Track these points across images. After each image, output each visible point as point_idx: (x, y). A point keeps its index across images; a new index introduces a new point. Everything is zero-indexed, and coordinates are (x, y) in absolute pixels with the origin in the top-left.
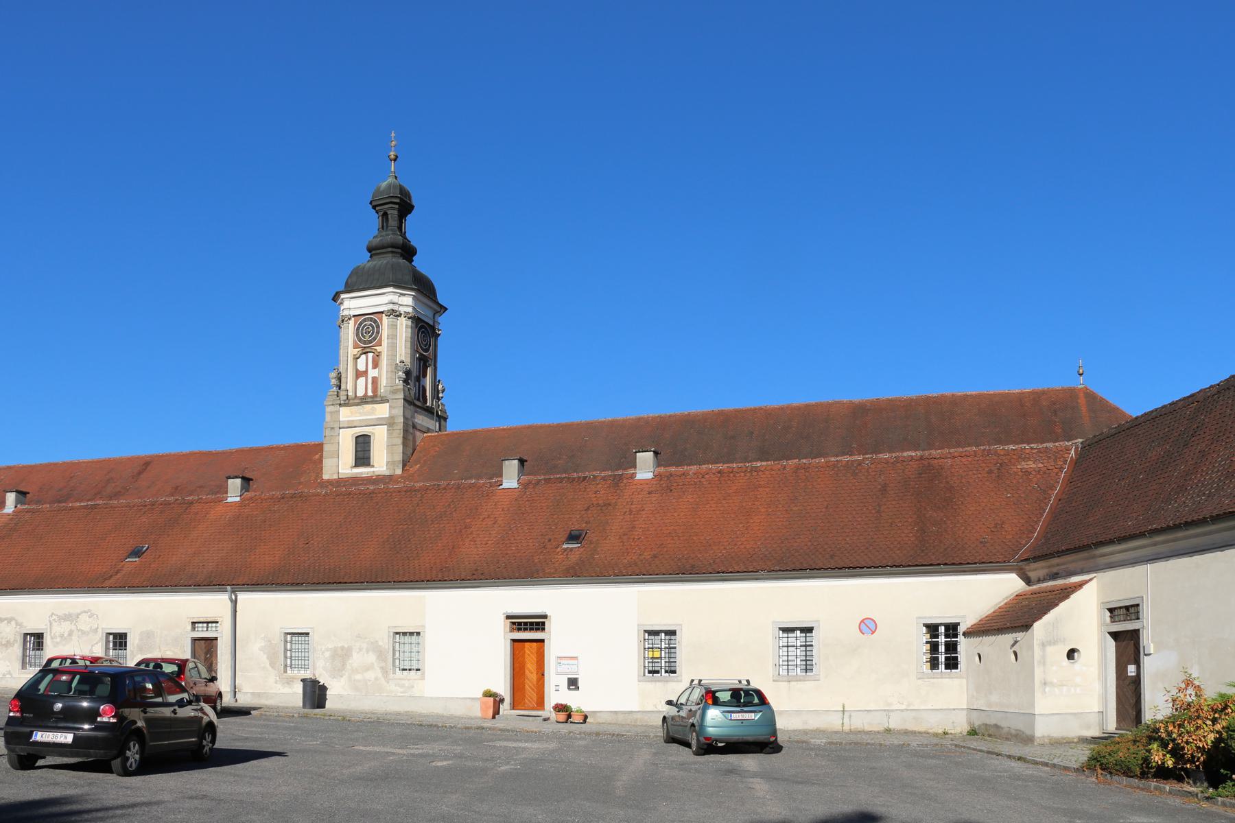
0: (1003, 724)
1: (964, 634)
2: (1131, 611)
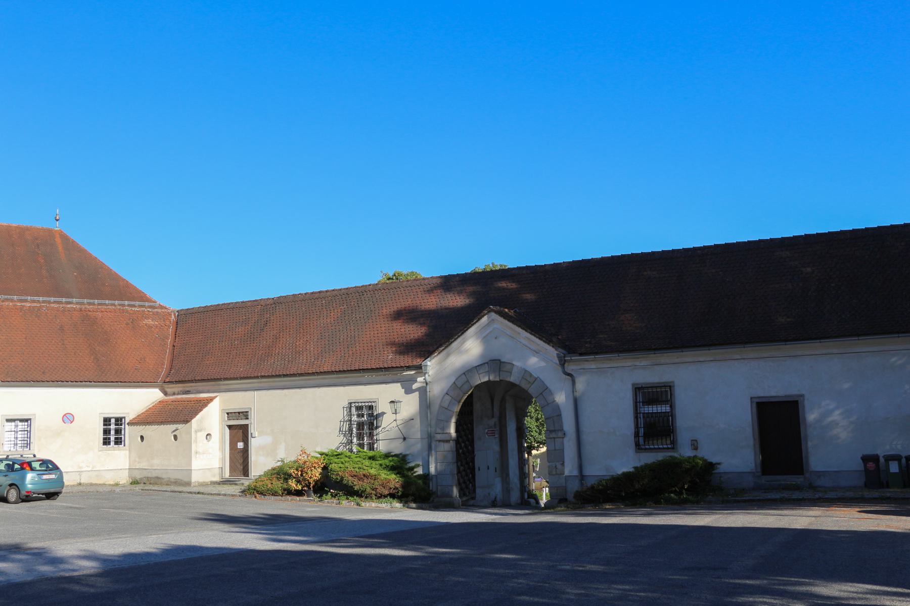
0: (164, 476)
1: (128, 424)
2: (245, 415)
